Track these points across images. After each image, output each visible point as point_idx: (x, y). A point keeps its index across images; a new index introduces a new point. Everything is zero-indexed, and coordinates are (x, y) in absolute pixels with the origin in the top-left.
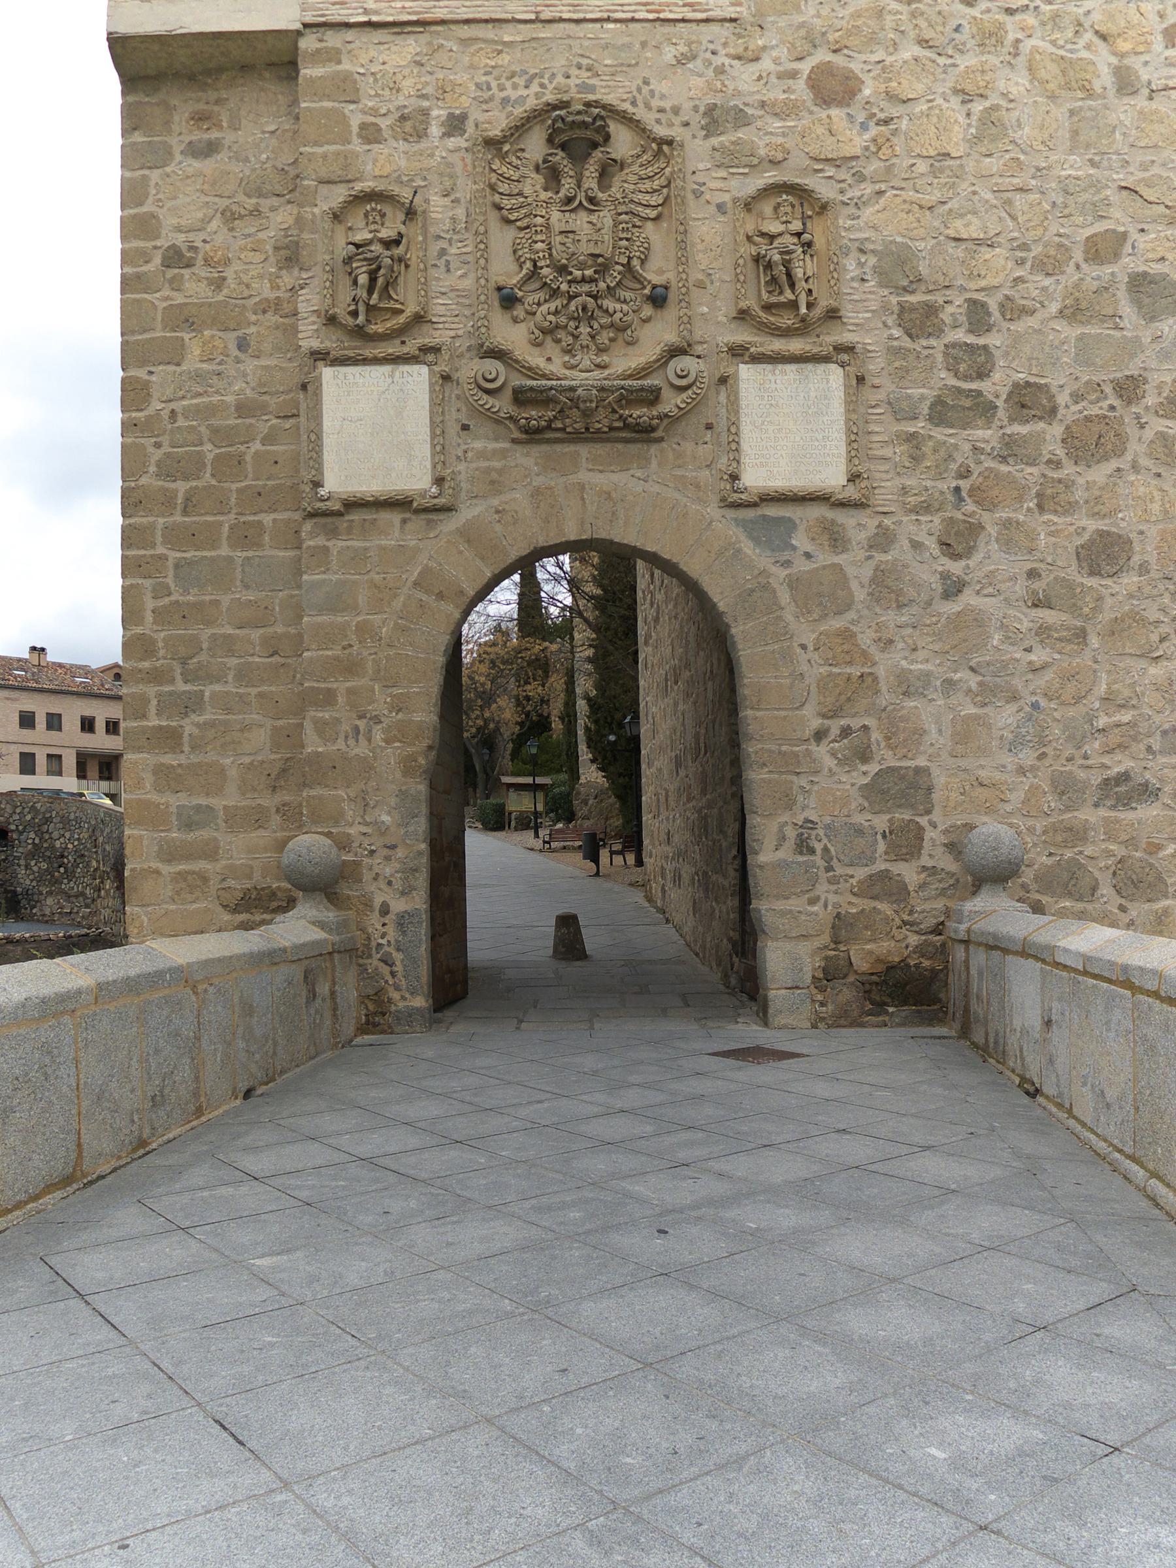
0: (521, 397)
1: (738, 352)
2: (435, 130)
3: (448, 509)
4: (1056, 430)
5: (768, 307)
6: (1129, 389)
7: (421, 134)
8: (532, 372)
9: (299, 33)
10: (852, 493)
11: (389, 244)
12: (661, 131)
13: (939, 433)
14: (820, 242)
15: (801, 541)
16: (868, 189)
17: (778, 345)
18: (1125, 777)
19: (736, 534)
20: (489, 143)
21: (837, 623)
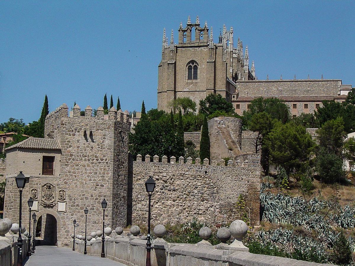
0: (44, 204)
1: (58, 201)
2: (39, 184)
3: (38, 211)
4: (79, 207)
5: (61, 198)
6: (85, 205)
7: (38, 185)
8: (45, 202)
9: (29, 177)
10: (65, 211)
11: (35, 193)
12: (54, 186)
13: (72, 207)
14: (64, 194)
15: (62, 214)
16: (67, 190)
17: (61, 201)
18: (82, 231)
19: (58, 214)
20: (42, 186)
21: (64, 220)
